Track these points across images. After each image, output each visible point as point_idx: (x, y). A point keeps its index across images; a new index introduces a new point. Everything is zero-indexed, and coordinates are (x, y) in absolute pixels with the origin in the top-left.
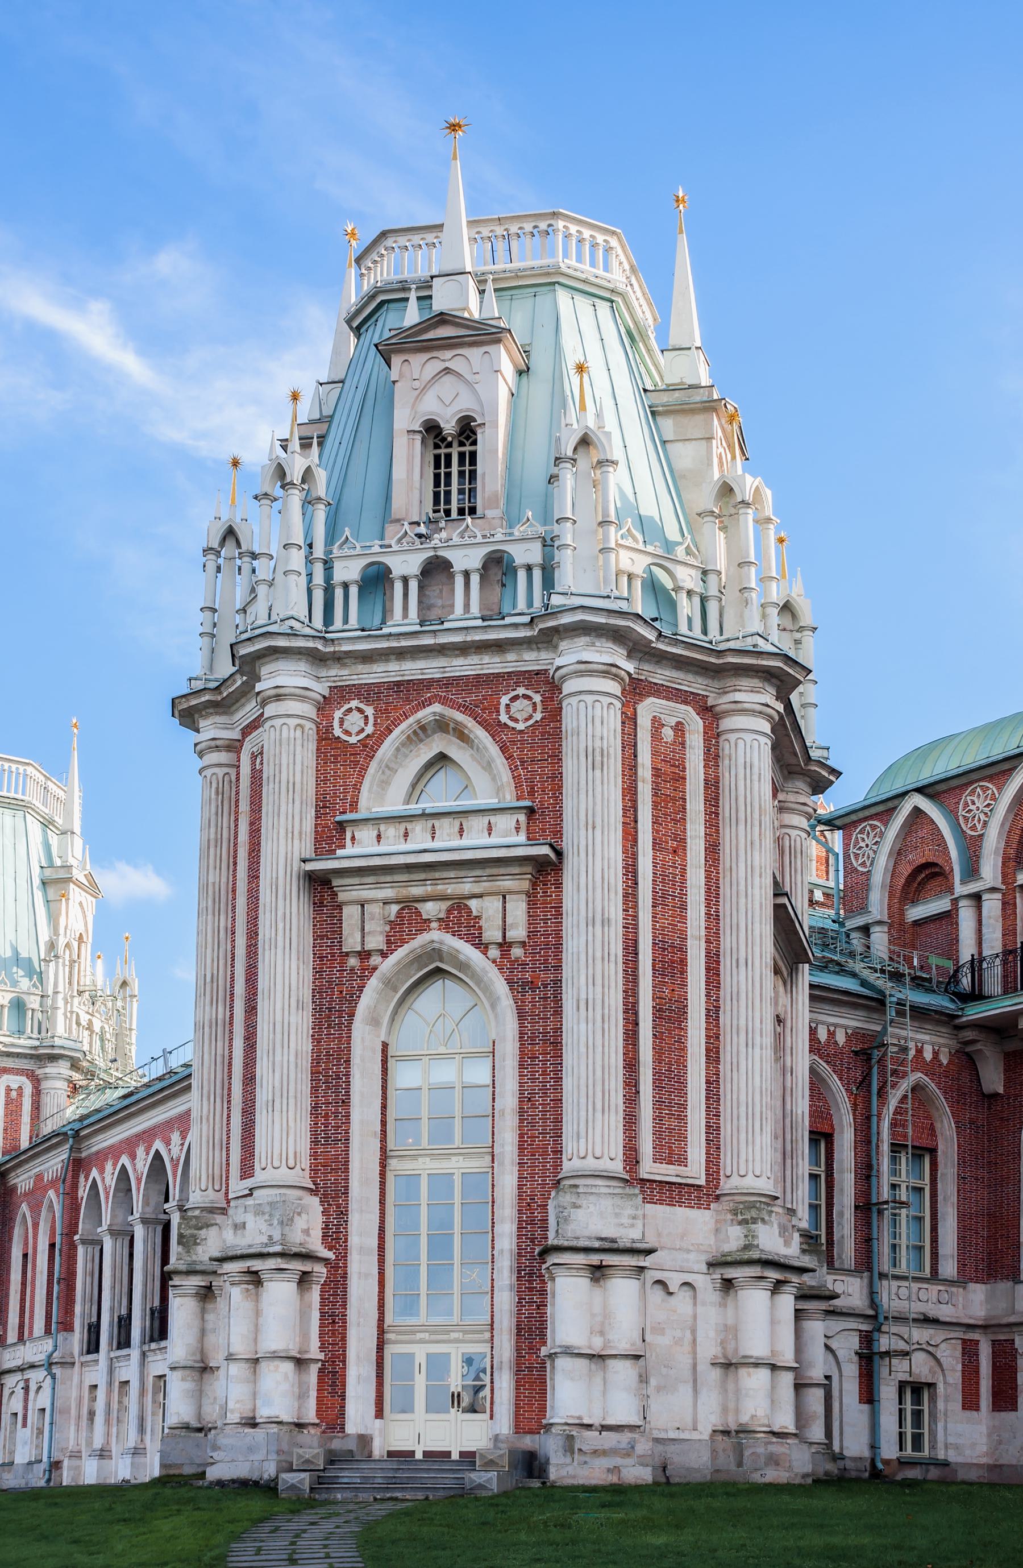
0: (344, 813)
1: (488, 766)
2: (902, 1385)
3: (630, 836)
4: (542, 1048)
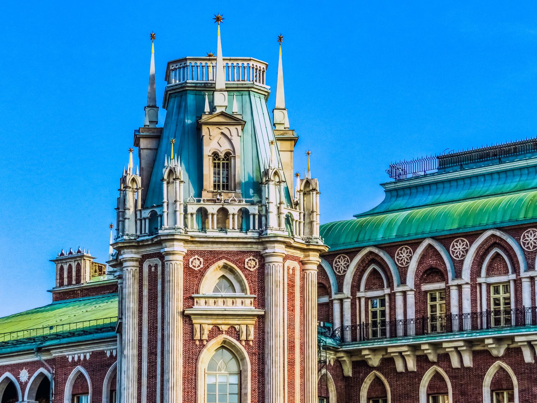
0: (193, 293)
1: (240, 282)
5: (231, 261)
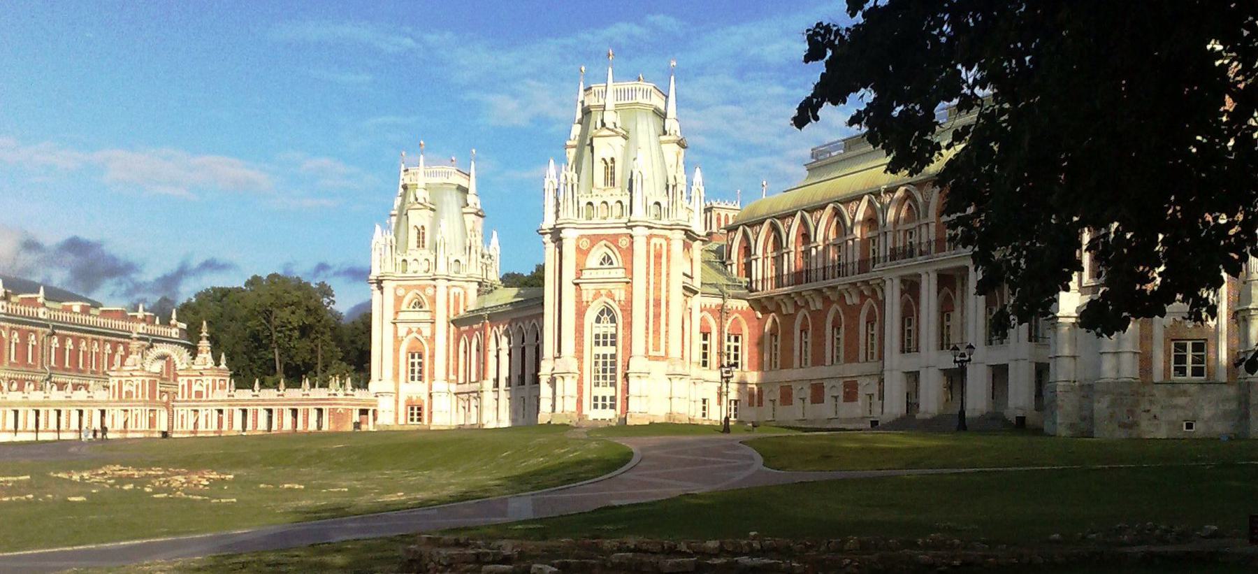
4: (629, 325)
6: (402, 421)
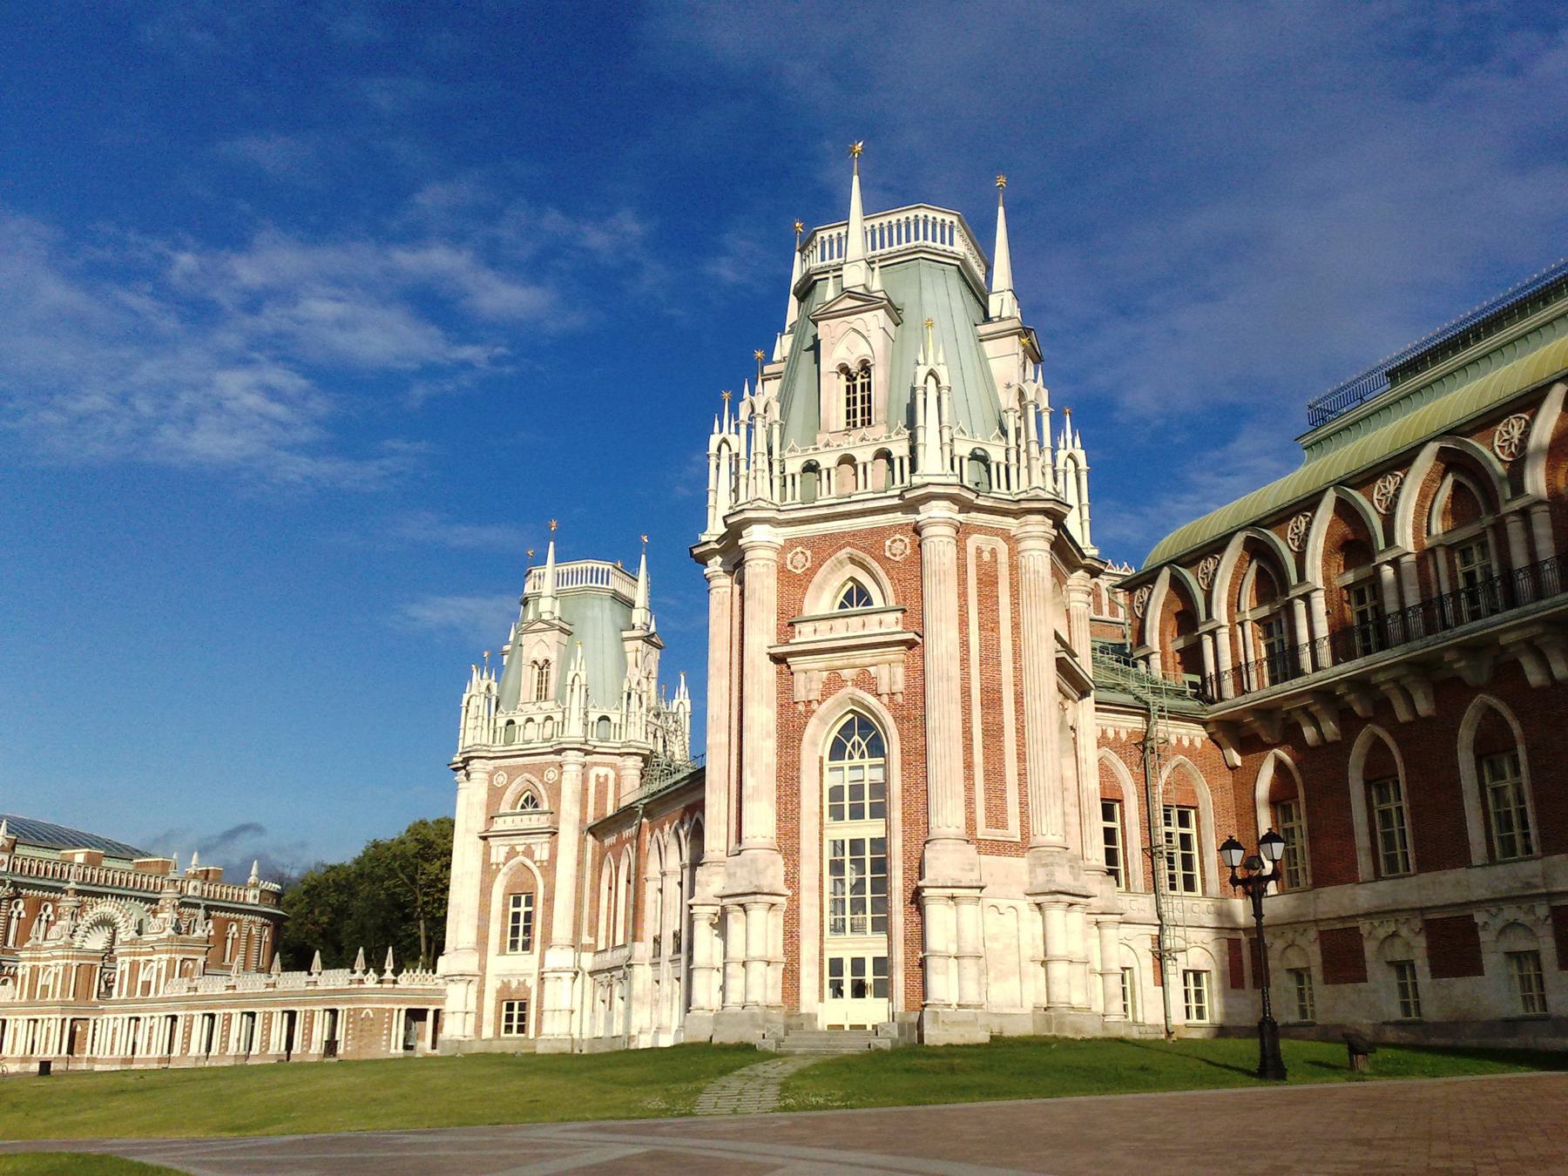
2: (1185, 973)
3: (963, 623)
4: (917, 757)
5: (863, 549)
6: (488, 1032)
